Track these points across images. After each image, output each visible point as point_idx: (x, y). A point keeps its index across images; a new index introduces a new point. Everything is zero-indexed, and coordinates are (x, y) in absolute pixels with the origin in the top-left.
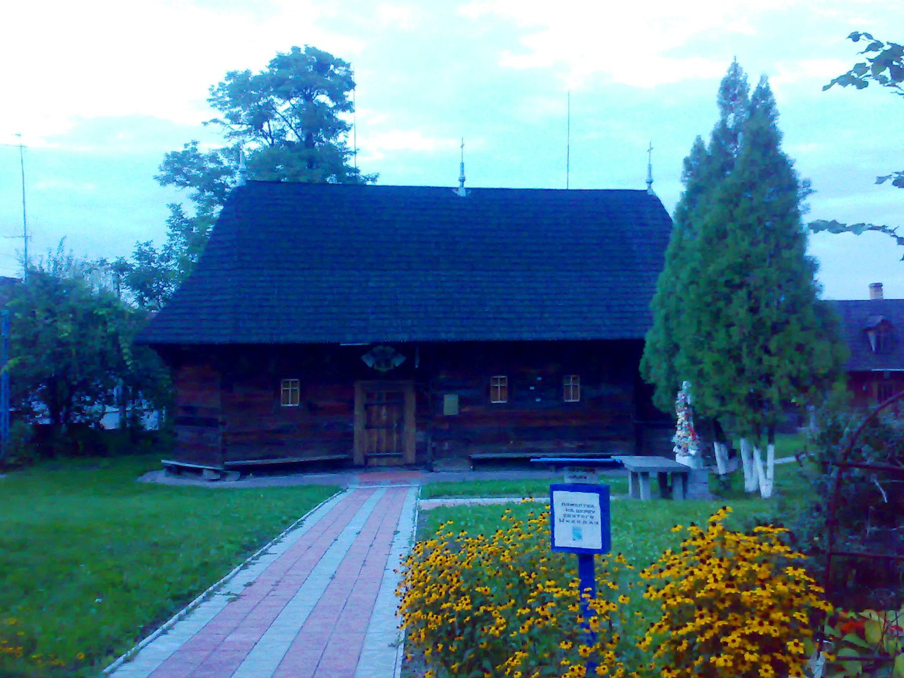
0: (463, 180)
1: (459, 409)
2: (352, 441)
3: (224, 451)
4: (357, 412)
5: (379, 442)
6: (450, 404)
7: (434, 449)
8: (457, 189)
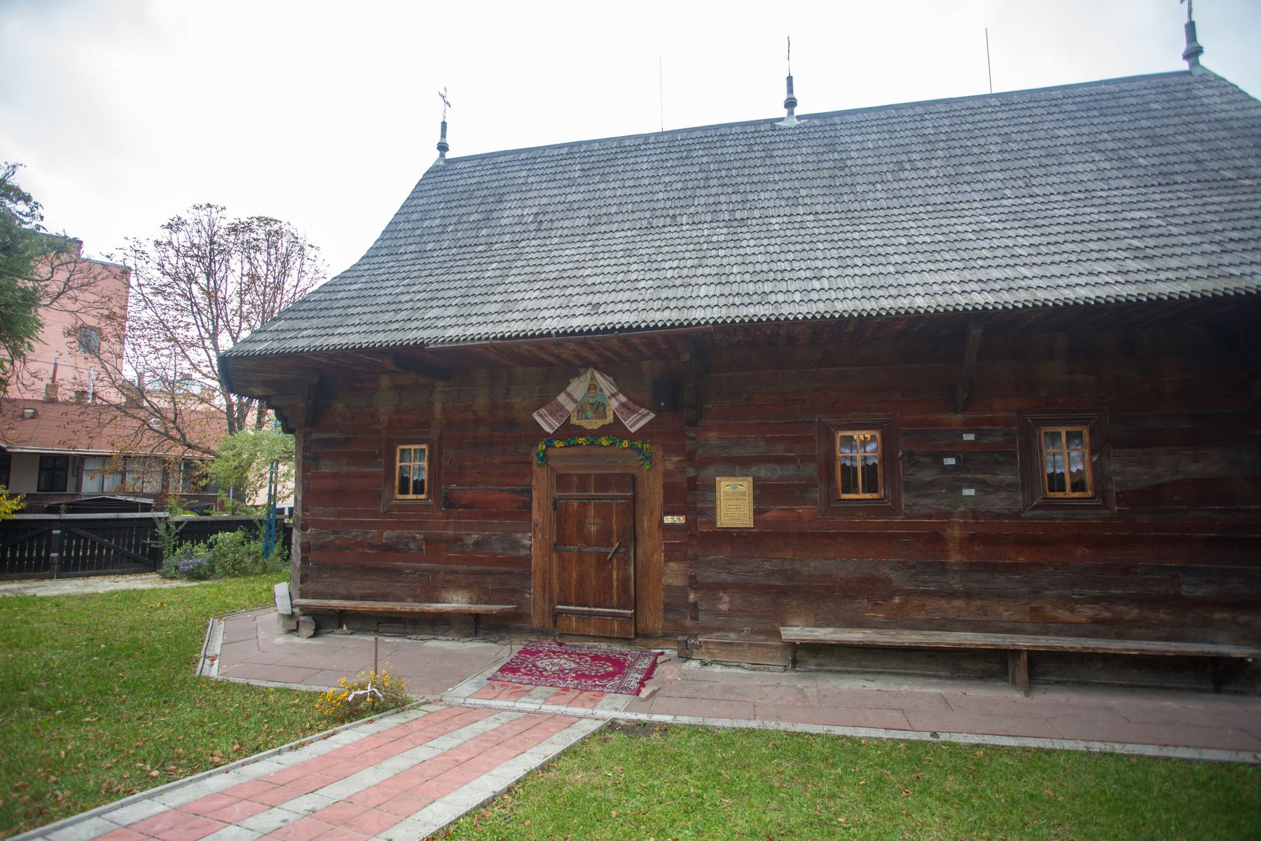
0: (791, 104)
1: (757, 512)
2: (527, 576)
4: (535, 515)
5: (581, 580)
6: (734, 501)
8: (781, 119)
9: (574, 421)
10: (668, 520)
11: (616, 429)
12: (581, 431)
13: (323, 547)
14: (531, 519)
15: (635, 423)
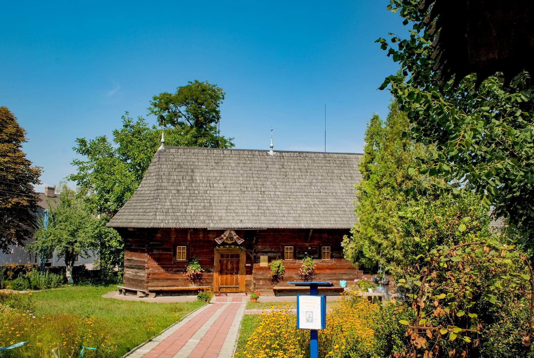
2: (212, 279)
3: (148, 282)
4: (215, 264)
7: (255, 284)
9: (225, 241)
10: (247, 265)
11: (235, 244)
12: (227, 244)
13: (154, 274)
14: (213, 265)
15: (240, 242)
